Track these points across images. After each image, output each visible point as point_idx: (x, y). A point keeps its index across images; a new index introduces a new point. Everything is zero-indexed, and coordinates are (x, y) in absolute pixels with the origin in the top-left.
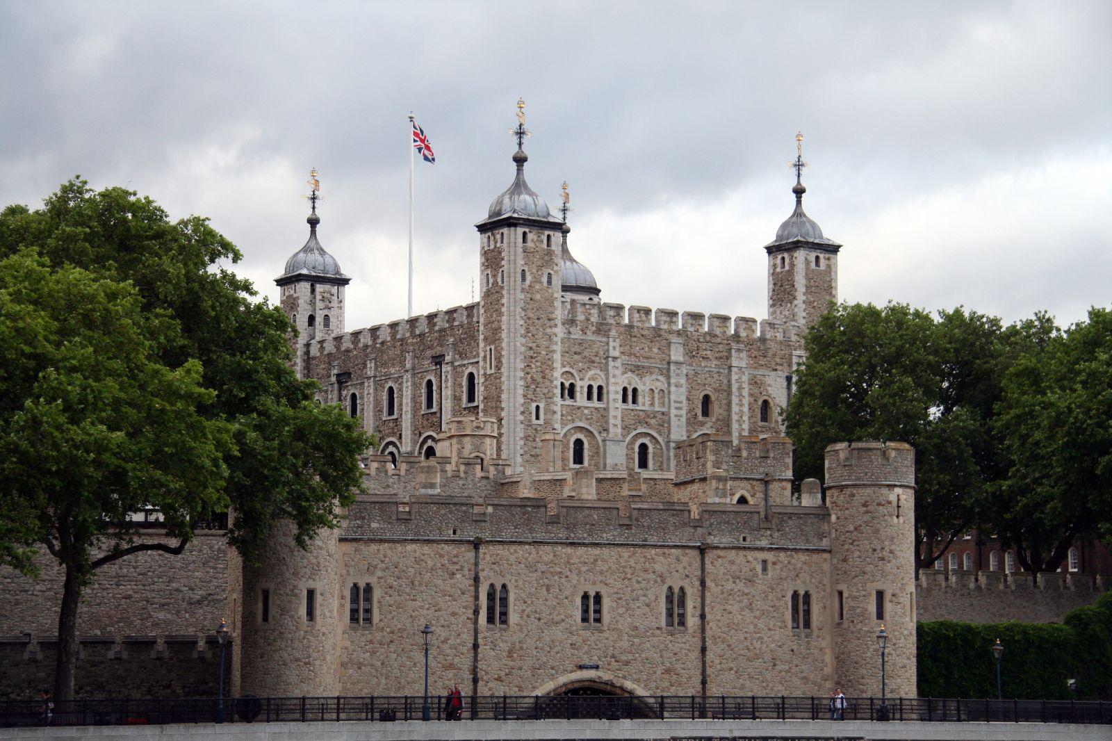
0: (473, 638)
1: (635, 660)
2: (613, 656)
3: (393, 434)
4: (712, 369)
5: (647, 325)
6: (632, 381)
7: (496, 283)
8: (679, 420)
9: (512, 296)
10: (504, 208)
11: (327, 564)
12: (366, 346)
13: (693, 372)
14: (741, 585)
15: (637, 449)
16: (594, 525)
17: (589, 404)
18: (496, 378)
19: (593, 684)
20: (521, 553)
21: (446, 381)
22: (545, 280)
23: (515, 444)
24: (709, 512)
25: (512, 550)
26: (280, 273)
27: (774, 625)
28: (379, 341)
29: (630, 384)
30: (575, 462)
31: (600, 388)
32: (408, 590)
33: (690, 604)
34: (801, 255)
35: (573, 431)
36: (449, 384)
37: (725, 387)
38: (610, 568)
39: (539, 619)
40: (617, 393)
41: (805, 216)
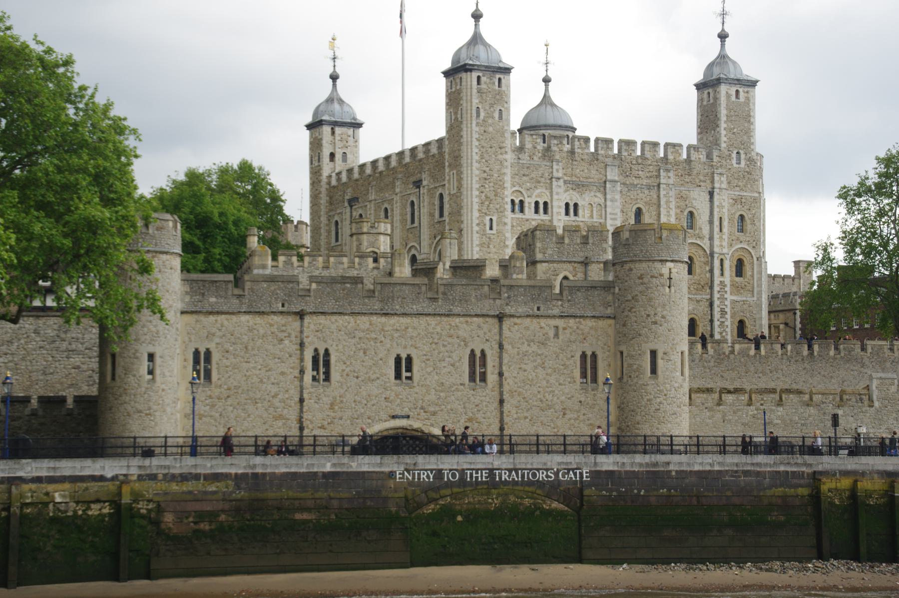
0: (299, 393)
1: (442, 410)
5: (586, 151)
6: (573, 197)
7: (456, 119)
11: (166, 332)
14: (534, 348)
16: (405, 298)
17: (536, 217)
18: (457, 197)
19: (405, 431)
20: (341, 322)
21: (423, 202)
22: (496, 115)
23: (472, 250)
25: (333, 320)
26: (309, 119)
27: (565, 380)
31: (545, 204)
32: (242, 354)
34: (723, 89)
36: (426, 204)
37: (655, 201)
38: (419, 334)
39: (357, 377)
40: (560, 207)
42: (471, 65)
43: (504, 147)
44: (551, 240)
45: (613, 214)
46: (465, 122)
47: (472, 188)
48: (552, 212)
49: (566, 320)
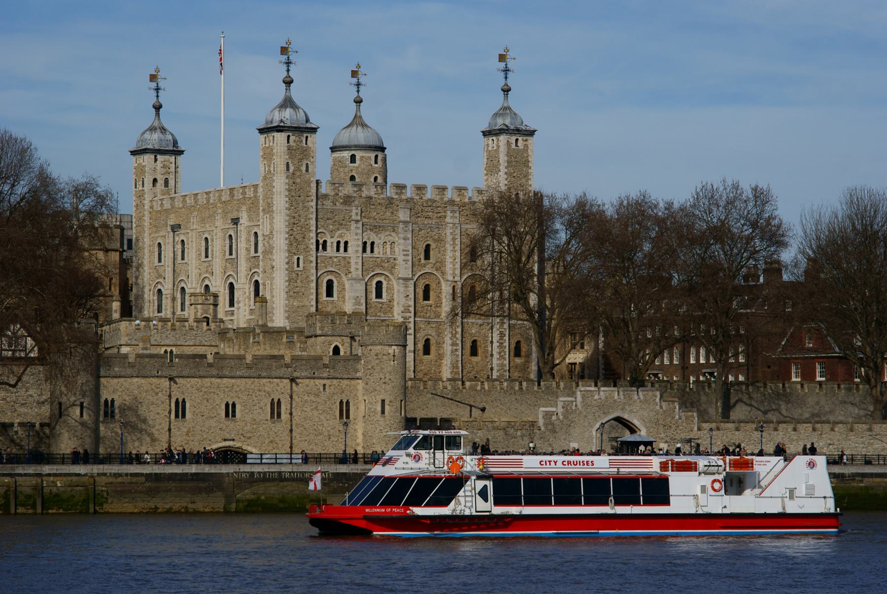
1: (254, 436)
2: (242, 434)
4: (432, 226)
5: (382, 196)
6: (371, 237)
8: (406, 263)
10: (275, 118)
13: (418, 229)
14: (312, 398)
15: (374, 286)
17: (338, 255)
21: (241, 237)
22: (304, 168)
24: (295, 359)
29: (369, 239)
33: (283, 408)
34: (503, 138)
35: (326, 274)
39: (203, 416)
40: (357, 246)
41: (509, 108)
42: (284, 127)
44: (327, 321)
45: (406, 251)
46: (276, 175)
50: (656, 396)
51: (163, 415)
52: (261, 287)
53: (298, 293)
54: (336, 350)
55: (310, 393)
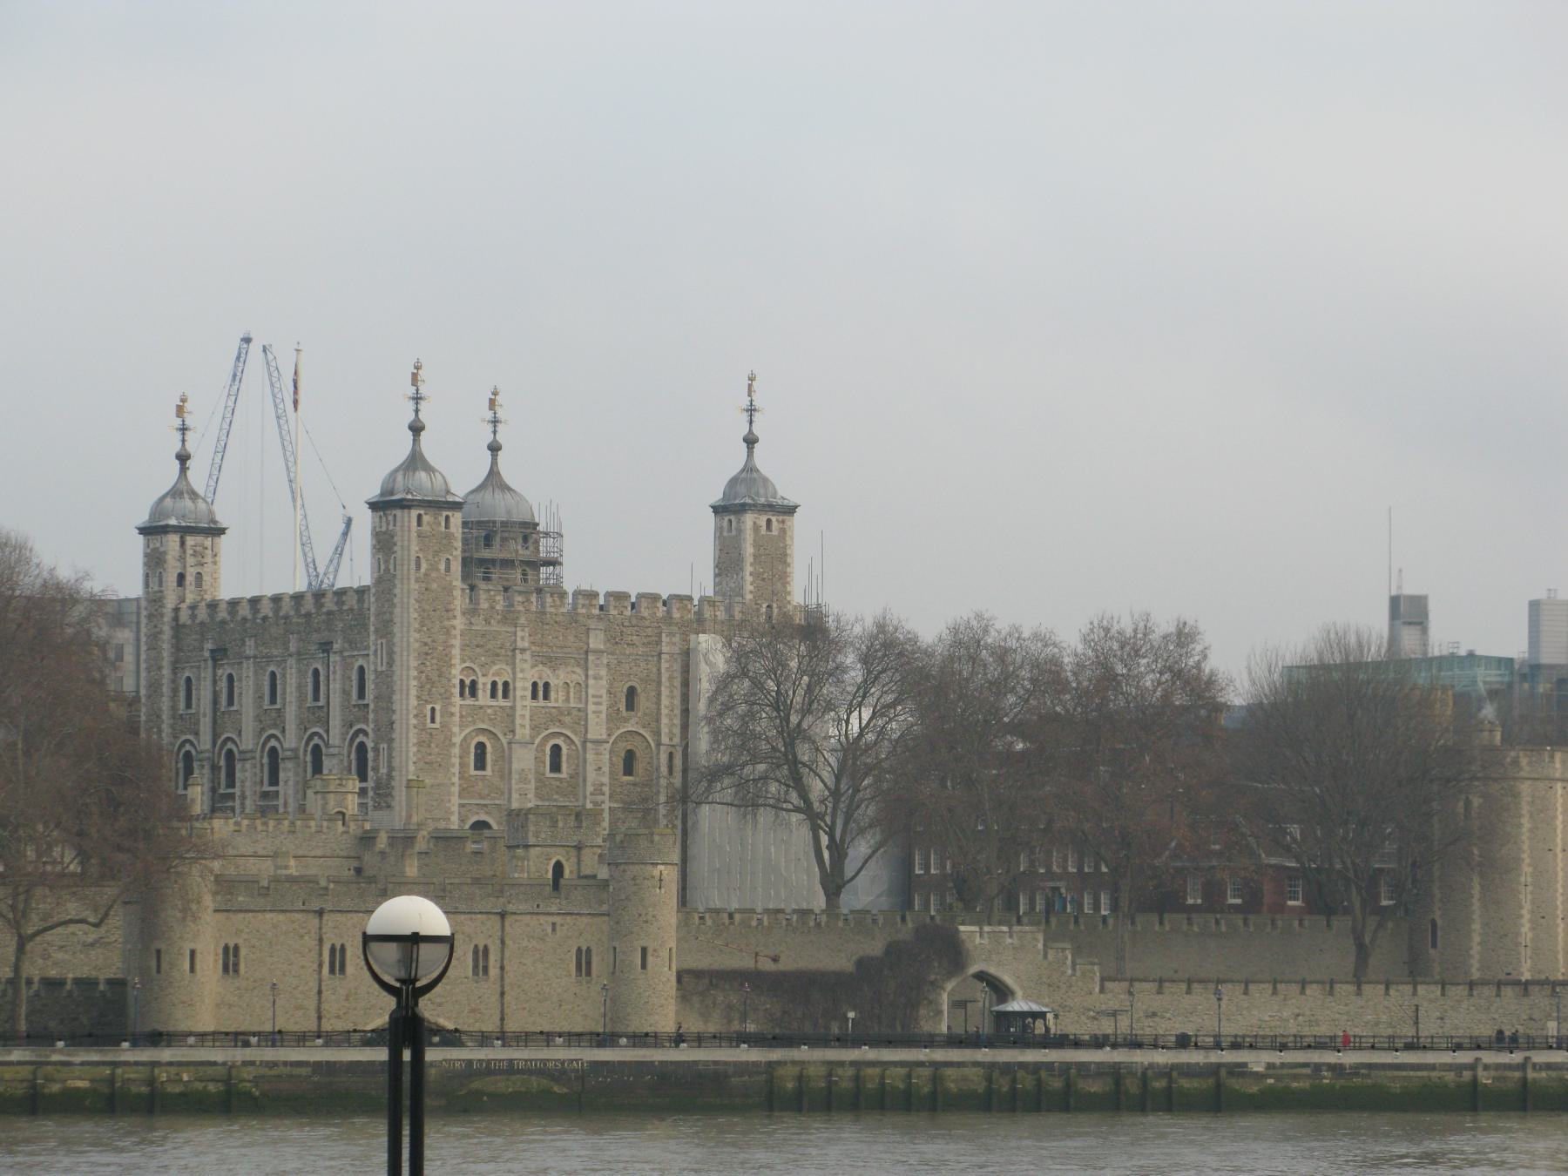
3: (275, 726)
7: (387, 570)
8: (598, 717)
9: (406, 587)
12: (245, 620)
14: (534, 943)
17: (493, 703)
18: (387, 676)
21: (334, 672)
22: (442, 567)
23: (407, 752)
28: (260, 616)
30: (476, 768)
31: (506, 684)
34: (749, 519)
35: (474, 734)
36: (338, 676)
37: (653, 676)
40: (525, 689)
42: (413, 500)
43: (452, 610)
46: (399, 577)
47: (408, 666)
48: (515, 697)
49: (564, 917)
50: (1037, 940)
51: (311, 970)
52: (370, 755)
53: (430, 763)
54: (558, 868)
55: (533, 937)
